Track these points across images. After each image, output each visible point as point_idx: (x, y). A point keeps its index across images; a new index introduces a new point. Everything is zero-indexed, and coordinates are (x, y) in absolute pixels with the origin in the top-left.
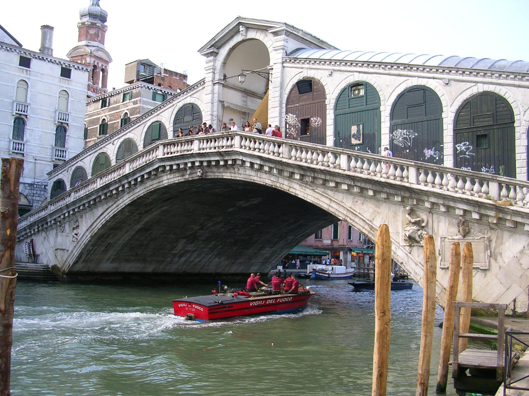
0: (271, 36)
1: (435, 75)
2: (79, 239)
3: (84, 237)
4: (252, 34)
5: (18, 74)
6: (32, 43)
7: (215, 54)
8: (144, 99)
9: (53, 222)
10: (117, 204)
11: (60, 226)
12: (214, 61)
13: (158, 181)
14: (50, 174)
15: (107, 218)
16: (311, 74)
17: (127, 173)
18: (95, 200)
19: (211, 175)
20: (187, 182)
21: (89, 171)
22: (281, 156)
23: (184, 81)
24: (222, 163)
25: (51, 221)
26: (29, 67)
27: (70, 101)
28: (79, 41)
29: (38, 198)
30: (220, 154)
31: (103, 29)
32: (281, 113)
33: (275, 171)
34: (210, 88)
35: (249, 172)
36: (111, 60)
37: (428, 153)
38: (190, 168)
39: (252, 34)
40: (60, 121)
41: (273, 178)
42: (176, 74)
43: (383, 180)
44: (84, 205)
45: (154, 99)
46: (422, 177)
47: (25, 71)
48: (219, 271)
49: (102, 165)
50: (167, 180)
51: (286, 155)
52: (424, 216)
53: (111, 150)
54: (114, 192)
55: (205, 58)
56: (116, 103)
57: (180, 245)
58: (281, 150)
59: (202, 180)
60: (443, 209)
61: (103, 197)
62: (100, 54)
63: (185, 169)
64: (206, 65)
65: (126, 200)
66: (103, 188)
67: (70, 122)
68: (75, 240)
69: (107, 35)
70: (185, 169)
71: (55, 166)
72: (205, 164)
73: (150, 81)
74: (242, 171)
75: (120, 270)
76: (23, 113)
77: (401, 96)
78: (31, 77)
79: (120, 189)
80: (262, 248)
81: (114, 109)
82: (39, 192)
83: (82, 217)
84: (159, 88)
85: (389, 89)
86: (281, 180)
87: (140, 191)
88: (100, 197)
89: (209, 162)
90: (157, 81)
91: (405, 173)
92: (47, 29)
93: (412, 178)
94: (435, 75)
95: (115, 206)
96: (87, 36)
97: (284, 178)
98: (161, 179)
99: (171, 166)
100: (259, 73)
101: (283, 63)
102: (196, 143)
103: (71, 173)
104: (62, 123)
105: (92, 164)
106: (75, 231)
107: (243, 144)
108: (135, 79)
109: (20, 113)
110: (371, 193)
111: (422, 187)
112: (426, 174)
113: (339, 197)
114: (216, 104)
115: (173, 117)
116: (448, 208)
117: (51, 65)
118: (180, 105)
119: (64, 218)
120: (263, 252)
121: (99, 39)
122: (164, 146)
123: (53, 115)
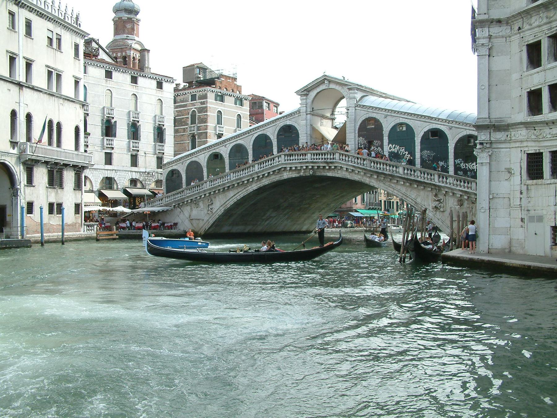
0: (348, 91)
1: (445, 124)
3: (219, 211)
4: (332, 86)
7: (307, 95)
8: (211, 100)
10: (246, 189)
11: (195, 204)
12: (306, 99)
13: (280, 175)
15: (239, 198)
16: (374, 115)
18: (229, 187)
19: (318, 174)
20: (301, 177)
23: (235, 83)
24: (327, 168)
27: (163, 107)
29: (149, 183)
30: (327, 163)
32: (355, 136)
33: (362, 173)
34: (305, 116)
35: (344, 173)
37: (441, 163)
38: (304, 169)
39: (332, 86)
41: (359, 177)
42: (229, 78)
43: (422, 180)
44: (219, 190)
46: (441, 179)
48: (284, 230)
50: (286, 175)
51: (368, 165)
52: (441, 197)
54: (246, 182)
55: (299, 96)
57: (268, 213)
58: (365, 163)
59: (311, 176)
60: (451, 194)
61: (236, 185)
63: (301, 170)
65: (254, 187)
66: (237, 180)
67: (165, 123)
68: (209, 212)
70: (301, 170)
73: (210, 83)
74: (339, 172)
75: (231, 231)
77: (426, 133)
78: (139, 91)
79: (251, 180)
80: (313, 213)
83: (215, 197)
84: (219, 90)
85: (420, 130)
86: (364, 178)
87: (266, 182)
88: (234, 185)
89: (318, 167)
90: (218, 84)
91: (432, 177)
93: (436, 180)
94: (445, 124)
95: (244, 190)
96: (124, 31)
97: (367, 177)
98: (282, 175)
99: (291, 168)
101: (355, 107)
102: (309, 155)
103: (186, 164)
105: (206, 160)
106: (210, 207)
107: (341, 157)
109: (134, 119)
110: (416, 186)
111: (441, 184)
112: (443, 178)
113: (399, 187)
114: (309, 127)
115: (276, 132)
116: (453, 193)
117: (150, 80)
118: (282, 124)
120: (314, 215)
121: (135, 32)
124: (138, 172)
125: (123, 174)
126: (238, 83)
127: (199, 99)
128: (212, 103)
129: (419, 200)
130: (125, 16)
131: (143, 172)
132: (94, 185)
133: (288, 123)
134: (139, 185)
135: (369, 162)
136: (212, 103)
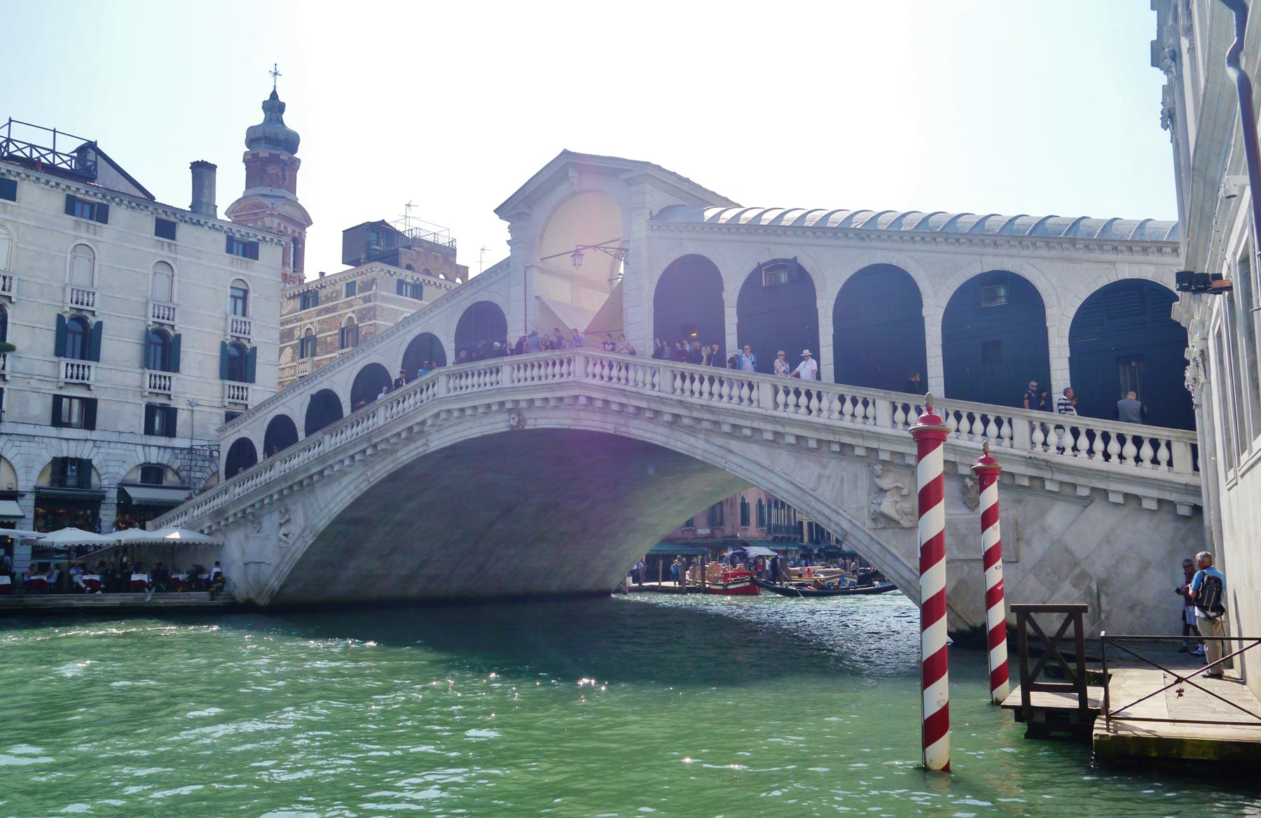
2: (291, 543)
5: (154, 251)
6: (174, 192)
9: (239, 515)
14: (221, 430)
17: (381, 423)
21: (300, 423)
22: (657, 388)
25: (235, 514)
26: (173, 238)
28: (247, 187)
29: (199, 475)
31: (295, 164)
36: (310, 223)
40: (238, 335)
44: (301, 482)
45: (399, 292)
47: (166, 246)
49: (324, 410)
53: (342, 384)
56: (328, 299)
62: (287, 210)
64: (509, 237)
69: (300, 175)
71: (230, 417)
72: (523, 405)
73: (391, 258)
76: (166, 321)
81: (327, 310)
82: (200, 463)
84: (409, 273)
87: (407, 454)
89: (531, 401)
90: (404, 260)
92: (203, 172)
100: (596, 247)
102: (506, 371)
104: (238, 338)
106: (283, 530)
108: (363, 256)
109: (160, 321)
117: (213, 233)
118: (466, 304)
119: (262, 506)
121: (287, 183)
122: (448, 376)
123: (222, 324)
124: (165, 448)
125: (118, 450)
126: (460, 260)
127: (363, 290)
128: (385, 299)
129: (826, 492)
130: (264, 152)
131: (182, 449)
132: (21, 477)
133: (483, 297)
134: (170, 478)
135: (669, 376)
136: (385, 299)
